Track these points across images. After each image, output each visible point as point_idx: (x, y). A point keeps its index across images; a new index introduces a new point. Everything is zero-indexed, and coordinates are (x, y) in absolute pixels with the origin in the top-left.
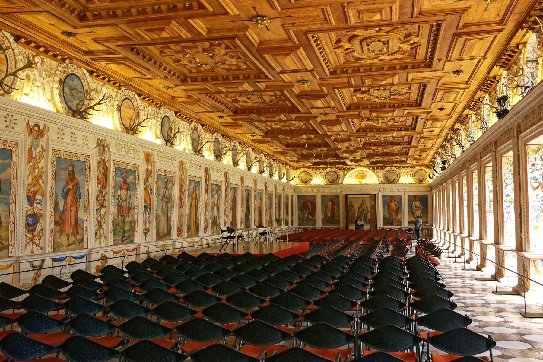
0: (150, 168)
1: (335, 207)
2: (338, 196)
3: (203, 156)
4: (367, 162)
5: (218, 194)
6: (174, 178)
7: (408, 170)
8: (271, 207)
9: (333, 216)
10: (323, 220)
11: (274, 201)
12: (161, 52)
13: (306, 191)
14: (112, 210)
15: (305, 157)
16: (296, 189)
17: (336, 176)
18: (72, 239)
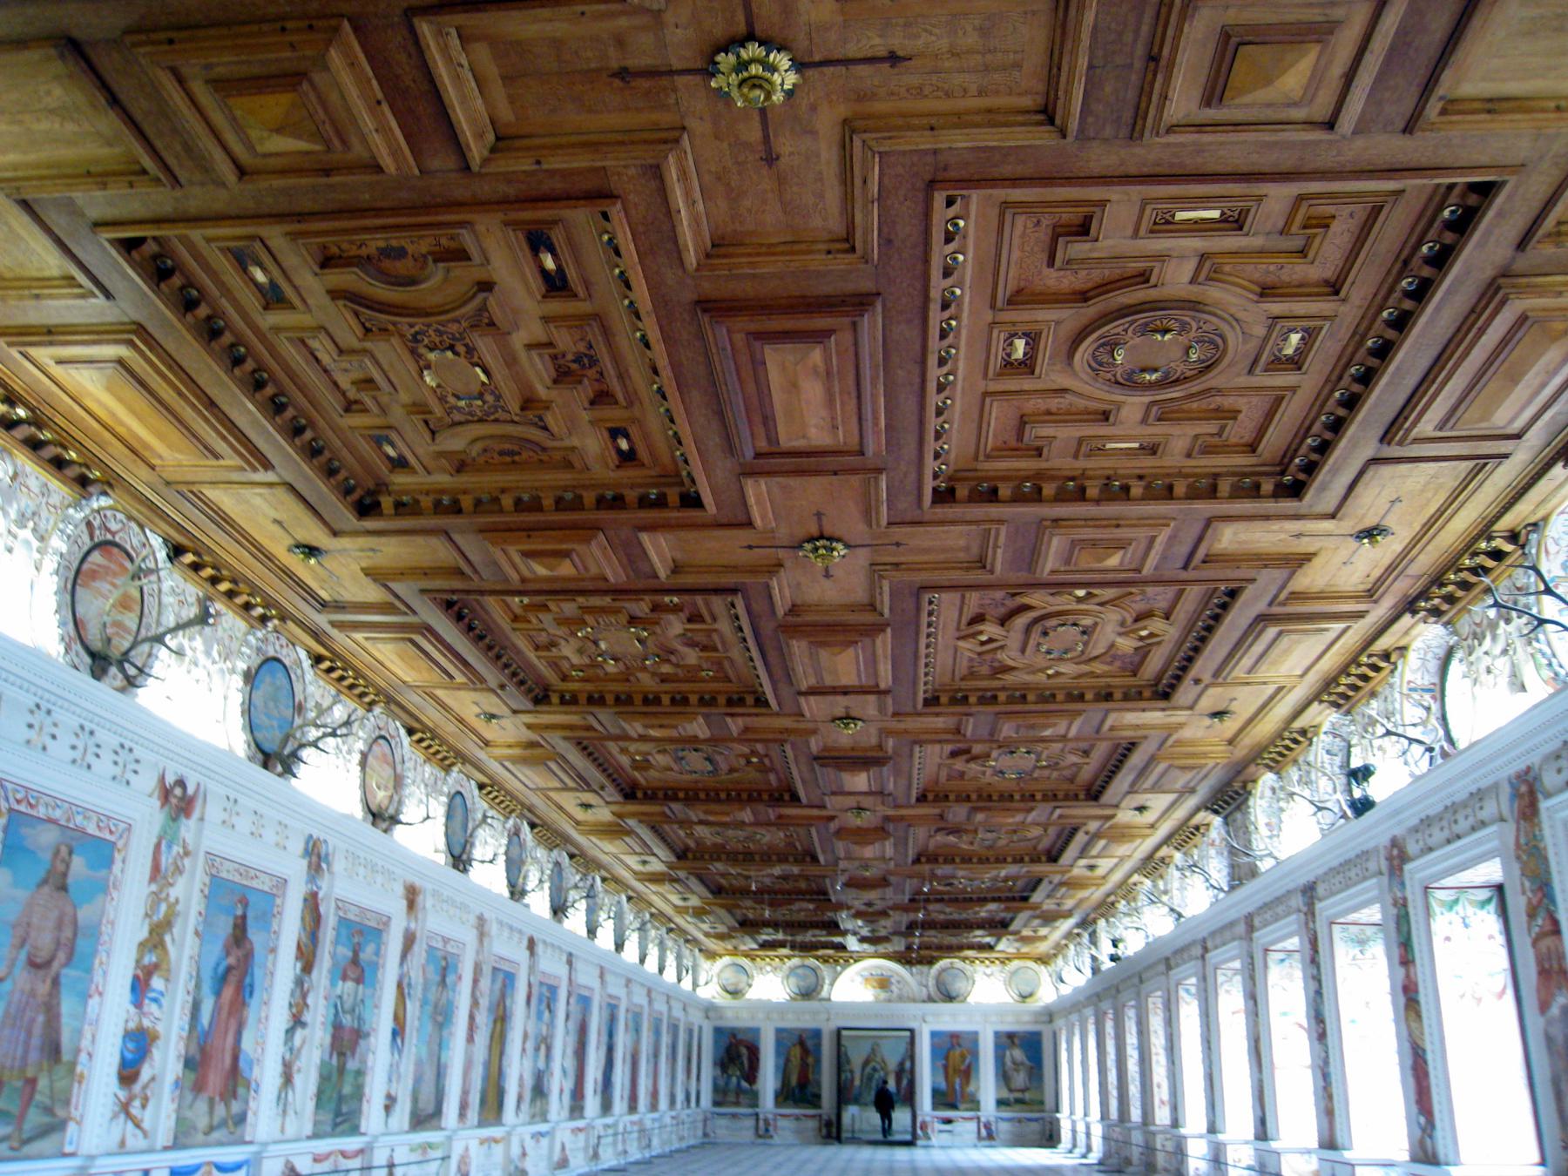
16: (709, 1009)
17: (812, 979)
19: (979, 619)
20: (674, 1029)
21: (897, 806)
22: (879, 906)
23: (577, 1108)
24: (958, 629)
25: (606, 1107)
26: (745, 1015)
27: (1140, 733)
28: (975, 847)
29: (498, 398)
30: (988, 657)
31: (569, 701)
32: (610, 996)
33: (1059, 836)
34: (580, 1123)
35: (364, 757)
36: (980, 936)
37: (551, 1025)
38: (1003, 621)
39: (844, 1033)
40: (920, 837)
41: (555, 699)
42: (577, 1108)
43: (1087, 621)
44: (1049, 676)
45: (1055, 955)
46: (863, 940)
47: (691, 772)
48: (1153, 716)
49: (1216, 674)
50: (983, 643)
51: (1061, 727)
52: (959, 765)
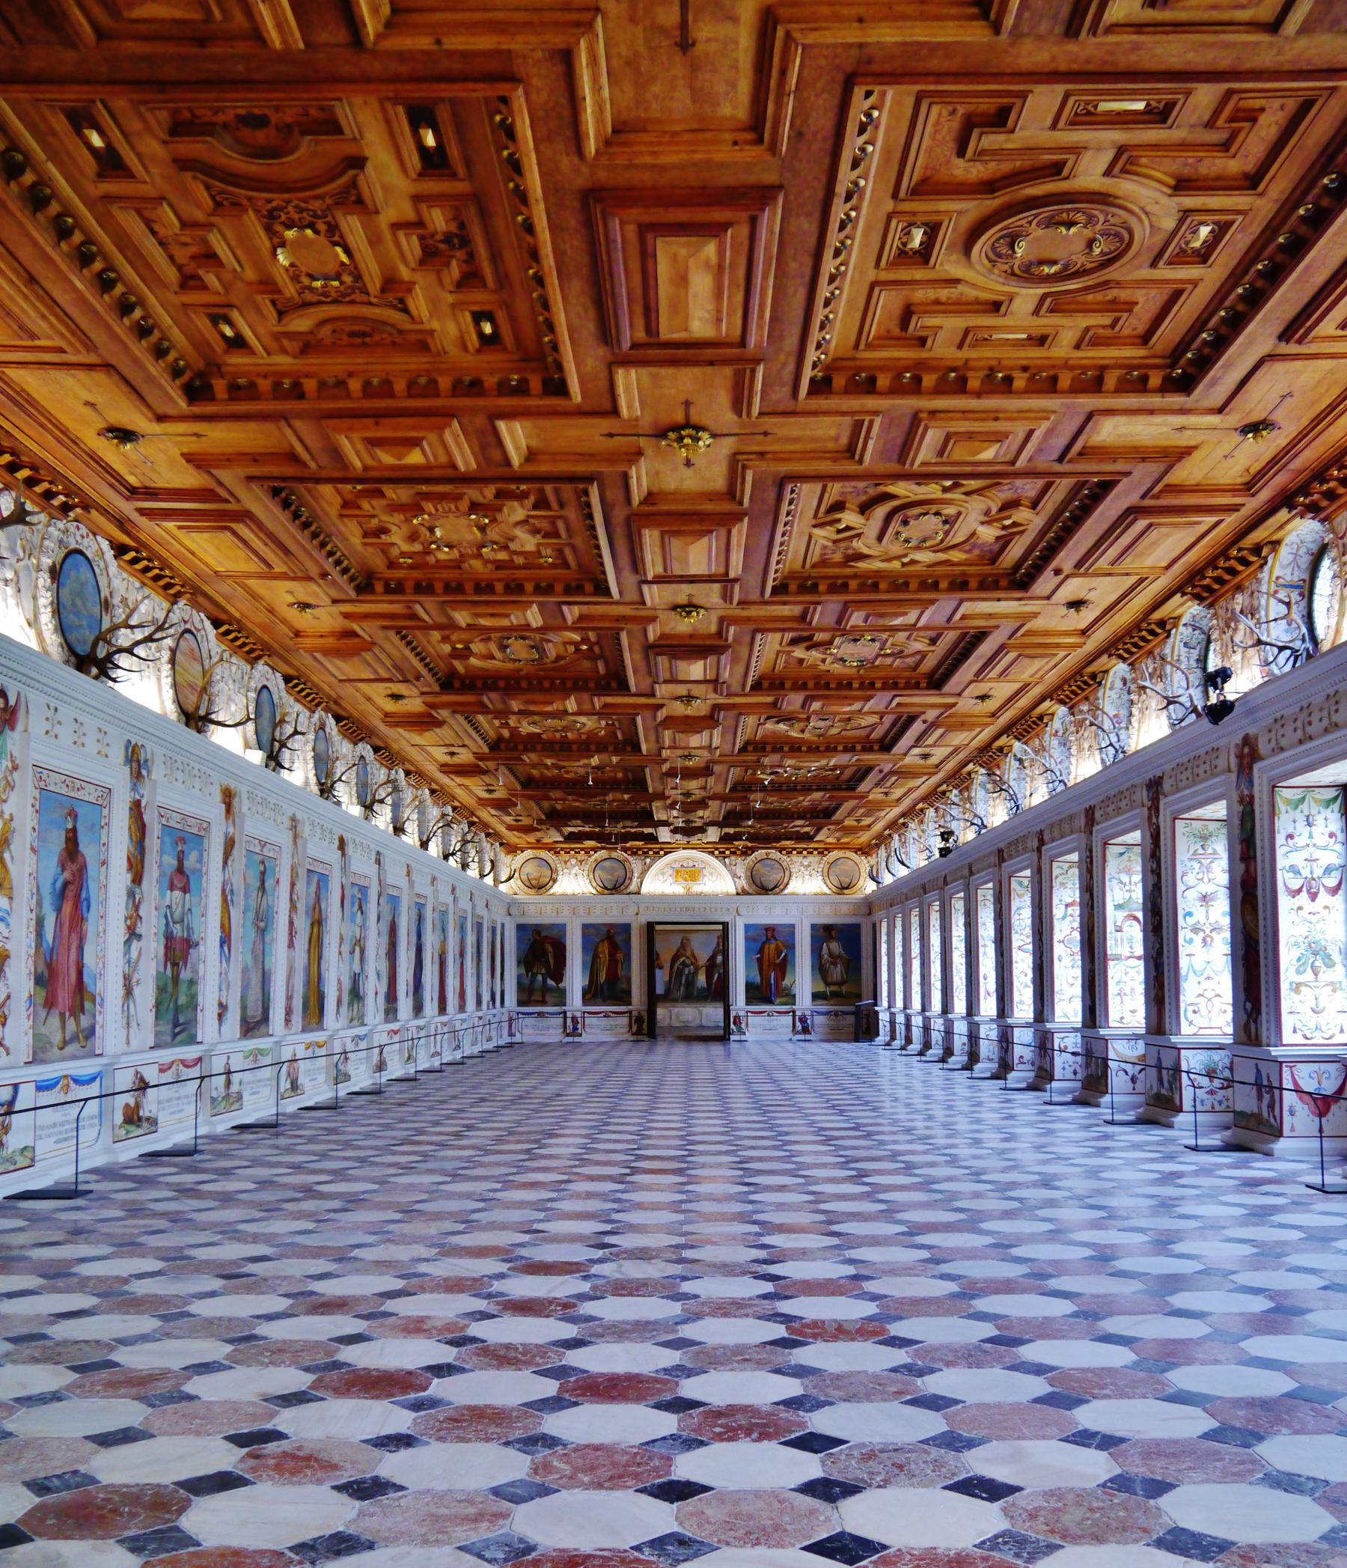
0: (231, 830)
2: (626, 928)
3: (338, 803)
4: (713, 834)
7: (811, 859)
8: (462, 954)
9: (613, 978)
10: (586, 992)
11: (486, 936)
12: (346, 504)
13: (540, 912)
14: (152, 946)
15: (555, 818)
16: (511, 905)
18: (71, 1024)
19: (839, 506)
20: (479, 926)
21: (729, 695)
22: (698, 794)
24: (815, 516)
25: (418, 1009)
26: (549, 909)
27: (992, 623)
28: (807, 735)
29: (358, 277)
30: (843, 545)
31: (395, 589)
32: (418, 895)
33: (894, 724)
35: (173, 652)
36: (800, 825)
37: (363, 927)
38: (864, 509)
41: (379, 587)
43: (950, 511)
44: (904, 565)
45: (878, 846)
46: (675, 831)
48: (1007, 606)
49: (1079, 565)
50: (839, 531)
51: (911, 617)
52: (799, 652)
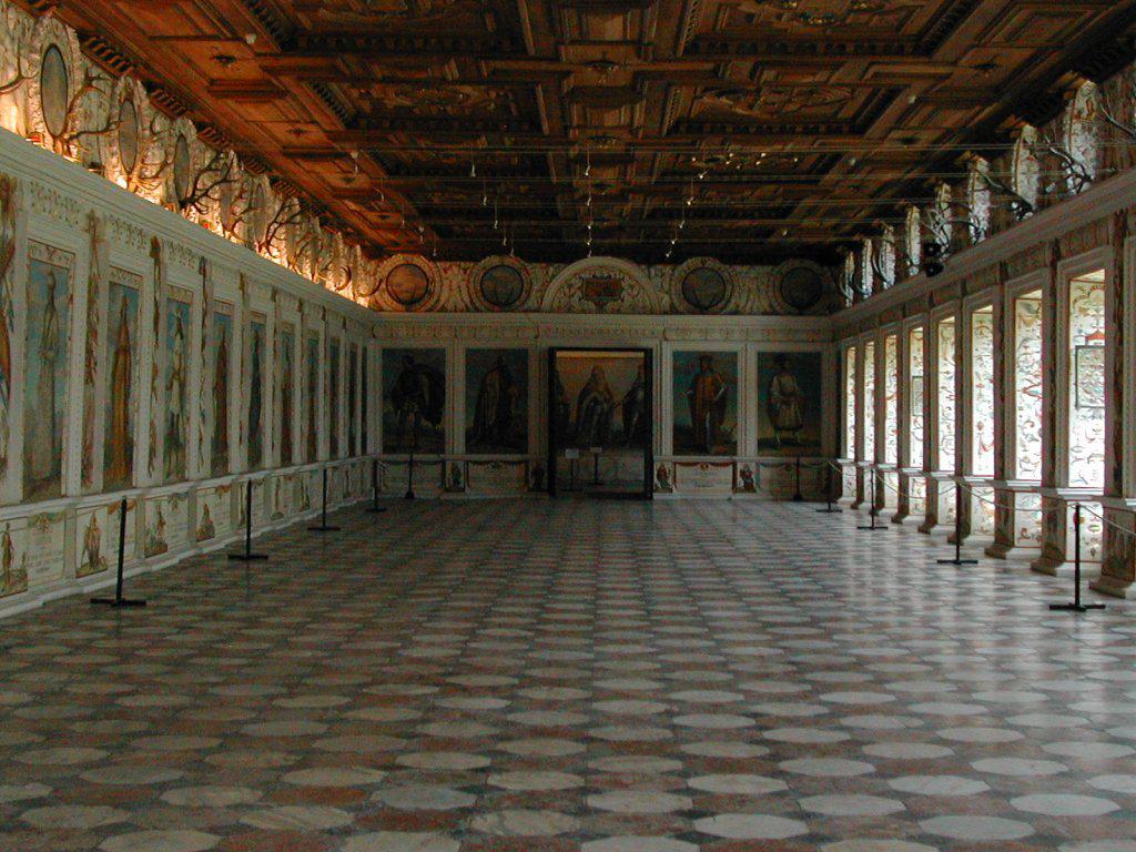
1: (513, 390)
2: (521, 355)
5: (182, 337)
6: (71, 273)
8: (312, 388)
10: (469, 437)
11: (343, 362)
23: (220, 463)
28: (756, 112)
32: (255, 314)
34: (226, 481)
39: (559, 354)
40: (682, 101)
42: (220, 463)
47: (378, 13)
